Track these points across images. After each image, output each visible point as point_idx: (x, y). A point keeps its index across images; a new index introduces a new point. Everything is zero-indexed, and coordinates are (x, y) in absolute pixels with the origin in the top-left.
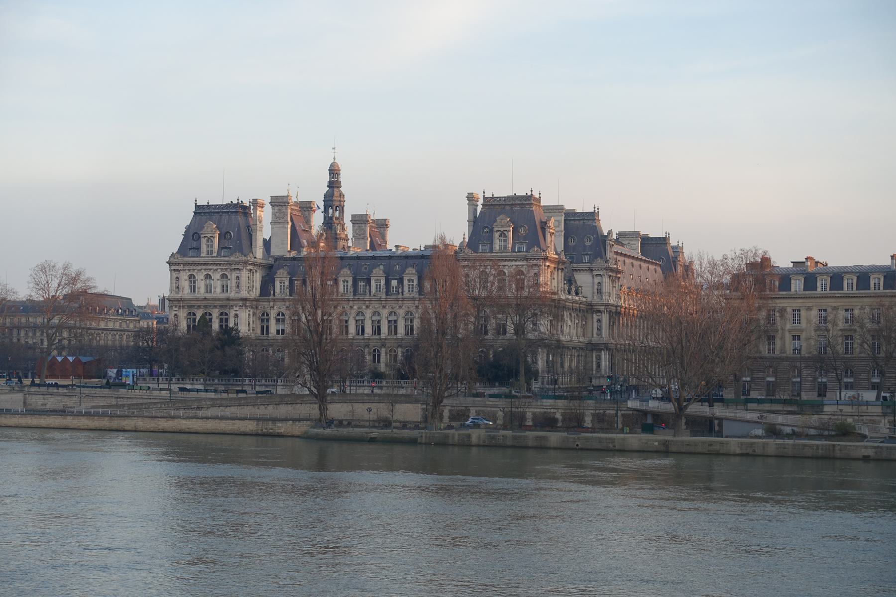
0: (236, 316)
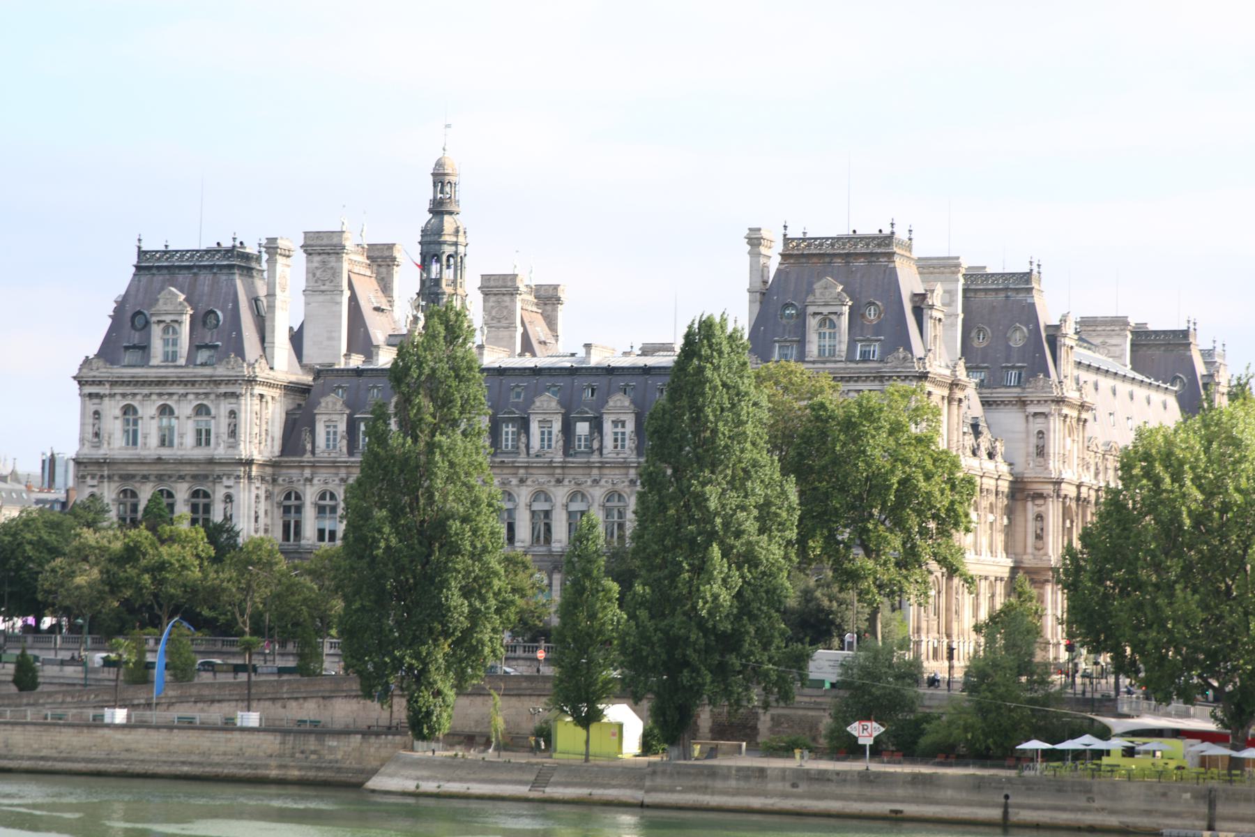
0: (229, 498)
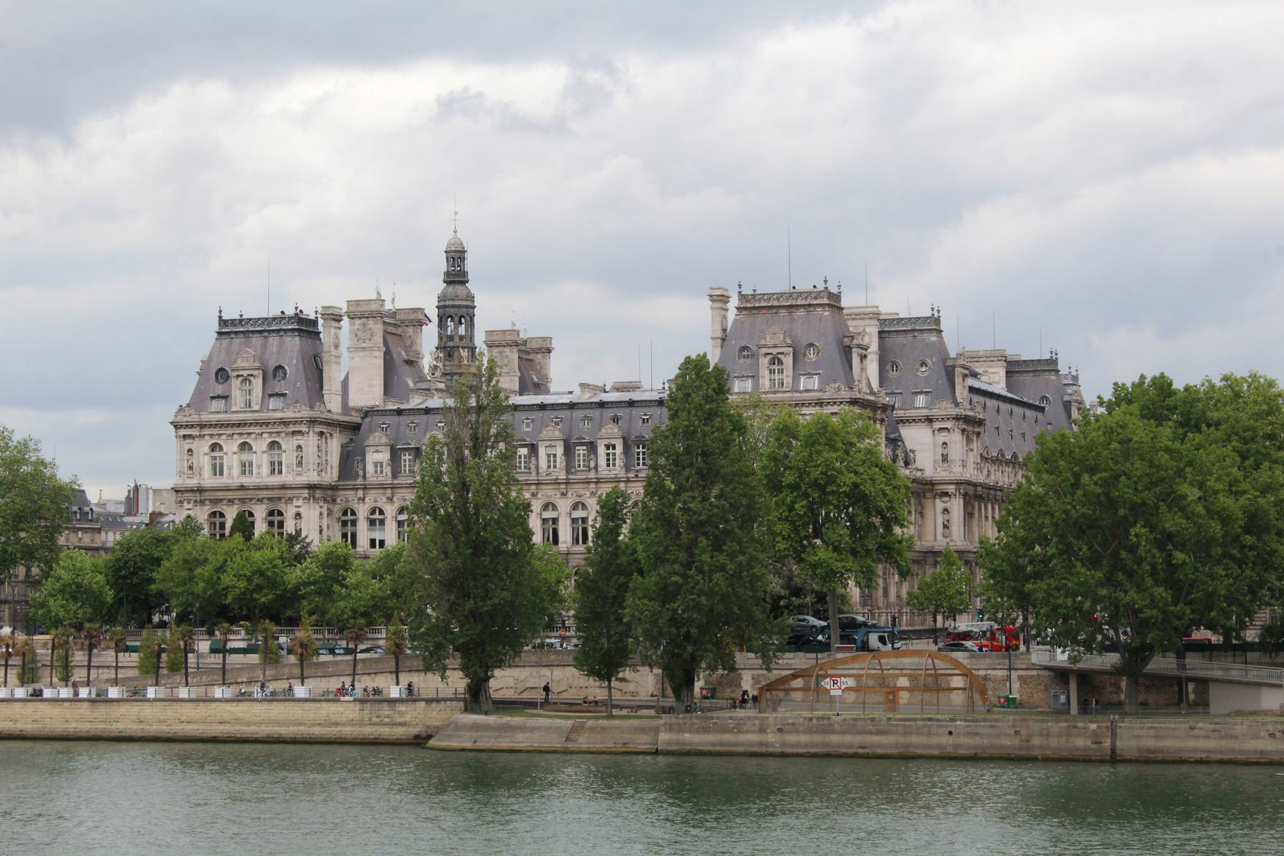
0: (298, 515)
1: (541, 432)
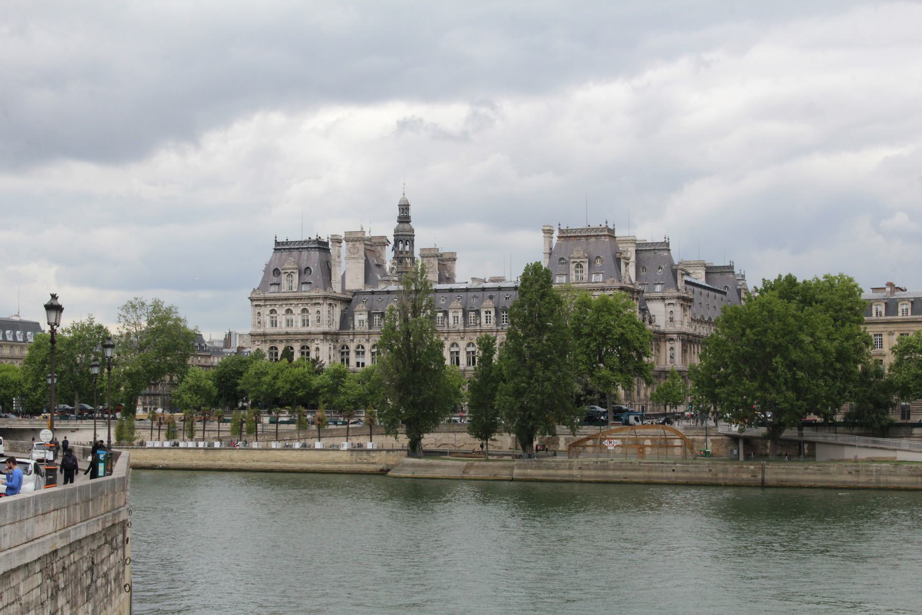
0: (318, 349)
1: (450, 304)
